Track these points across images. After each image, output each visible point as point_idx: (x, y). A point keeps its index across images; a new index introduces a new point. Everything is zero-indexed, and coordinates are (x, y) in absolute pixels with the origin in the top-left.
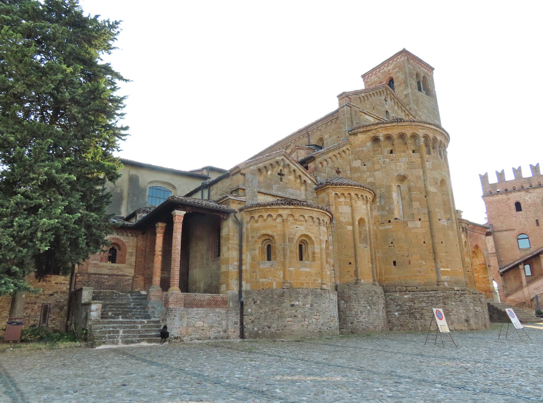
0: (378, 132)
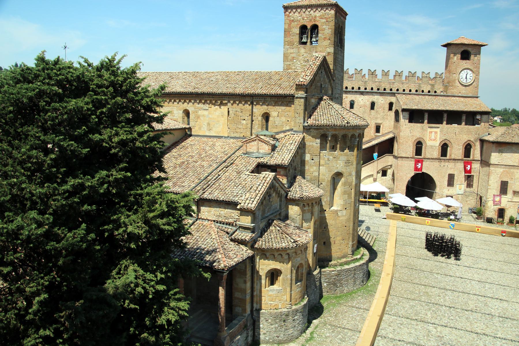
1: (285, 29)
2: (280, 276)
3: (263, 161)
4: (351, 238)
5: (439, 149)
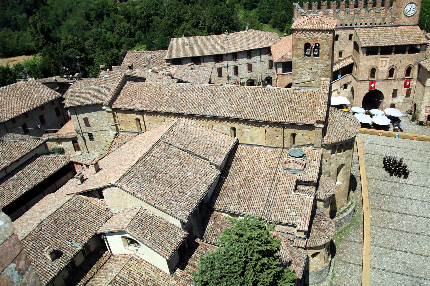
3: (299, 178)
5: (387, 73)
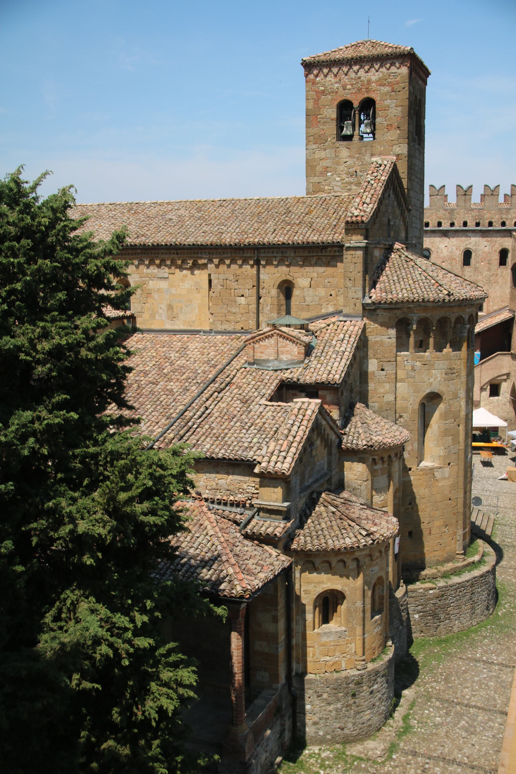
0: (412, 312)
1: (307, 110)
2: (342, 604)
3: (290, 376)
4: (461, 522)
